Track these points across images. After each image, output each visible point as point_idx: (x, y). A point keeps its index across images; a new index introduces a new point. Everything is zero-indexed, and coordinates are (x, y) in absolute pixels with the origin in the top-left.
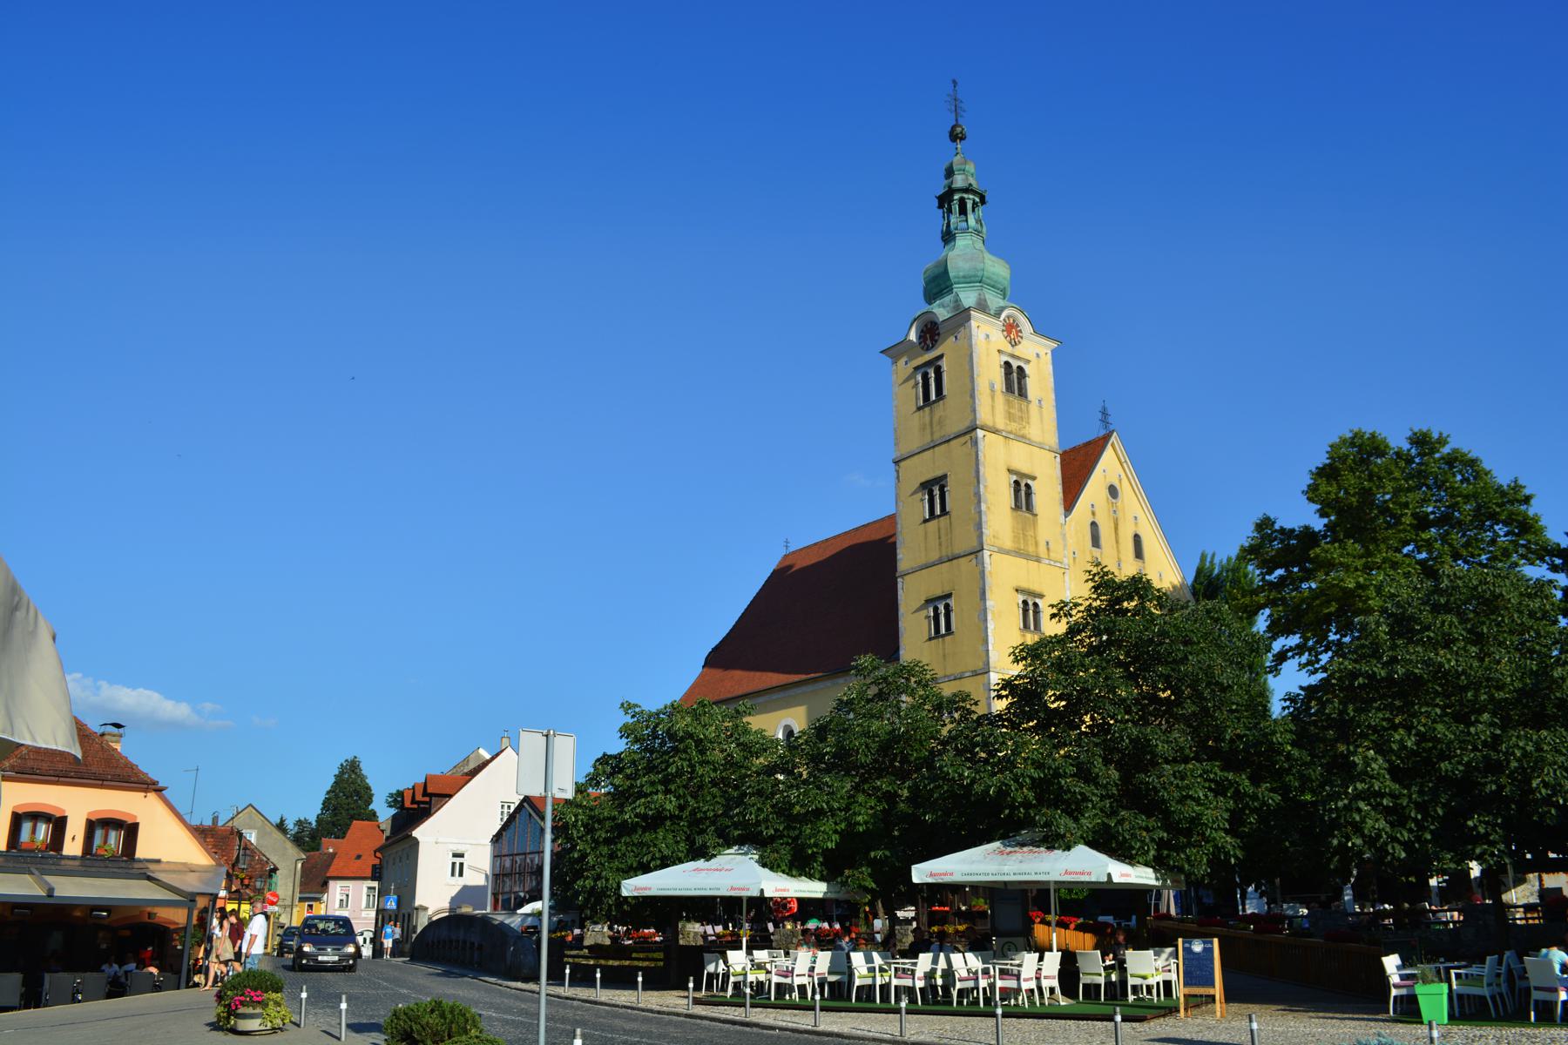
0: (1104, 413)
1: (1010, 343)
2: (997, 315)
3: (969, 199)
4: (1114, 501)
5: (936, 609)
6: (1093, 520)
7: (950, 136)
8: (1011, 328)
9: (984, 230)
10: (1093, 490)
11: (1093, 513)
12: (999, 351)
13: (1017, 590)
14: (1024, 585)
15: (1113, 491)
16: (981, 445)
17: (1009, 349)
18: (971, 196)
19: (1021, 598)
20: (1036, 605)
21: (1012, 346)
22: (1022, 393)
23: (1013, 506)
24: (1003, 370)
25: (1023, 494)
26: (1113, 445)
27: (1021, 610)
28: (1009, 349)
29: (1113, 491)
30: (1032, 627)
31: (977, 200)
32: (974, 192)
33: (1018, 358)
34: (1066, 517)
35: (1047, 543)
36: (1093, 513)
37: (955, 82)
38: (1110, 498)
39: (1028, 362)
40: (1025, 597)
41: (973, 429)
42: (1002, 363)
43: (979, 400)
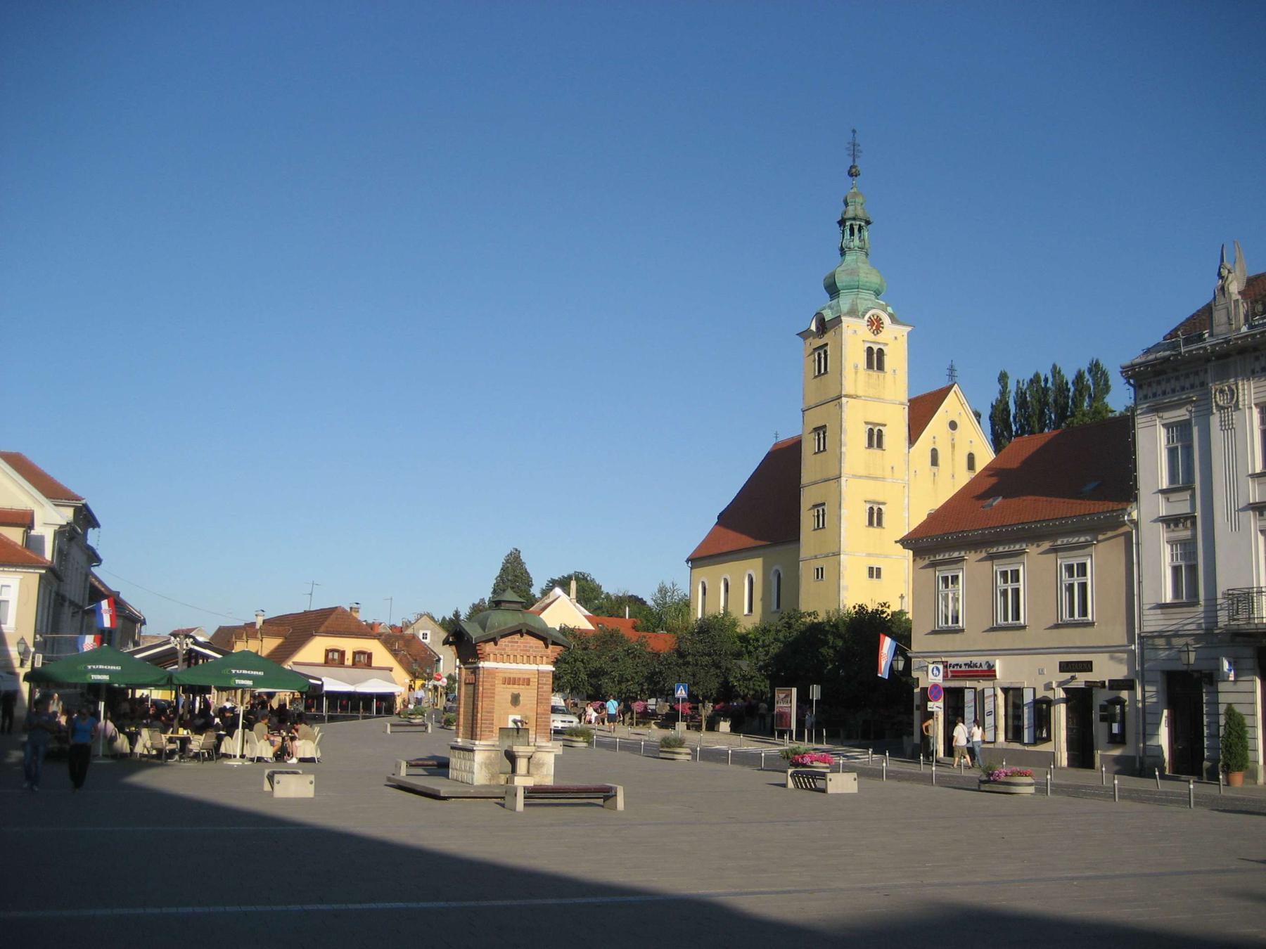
0: (952, 369)
1: (873, 333)
2: (863, 316)
3: (856, 225)
4: (954, 432)
7: (849, 173)
8: (876, 325)
9: (867, 246)
10: (937, 424)
12: (863, 341)
13: (865, 501)
15: (953, 425)
16: (845, 408)
18: (858, 223)
19: (869, 506)
20: (880, 509)
21: (875, 335)
23: (867, 446)
25: (875, 438)
26: (955, 392)
27: (867, 514)
28: (871, 337)
29: (953, 425)
30: (875, 525)
31: (863, 224)
32: (861, 220)
33: (879, 343)
34: (909, 448)
35: (892, 468)
36: (934, 443)
40: (871, 505)
41: (840, 397)
43: (845, 377)
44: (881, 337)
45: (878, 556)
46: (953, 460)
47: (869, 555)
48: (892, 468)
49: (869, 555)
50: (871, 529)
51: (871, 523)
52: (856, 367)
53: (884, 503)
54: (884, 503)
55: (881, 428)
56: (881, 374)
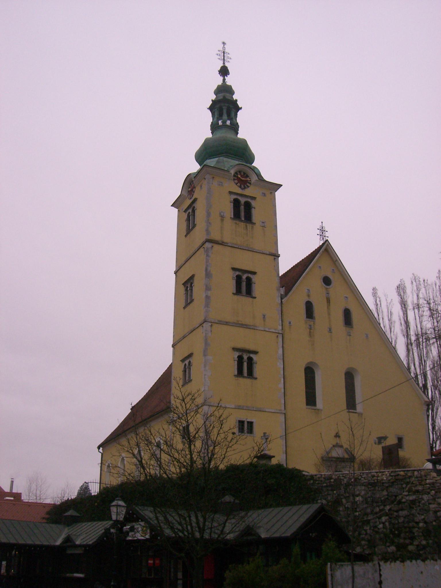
0: (322, 230)
4: (328, 287)
5: (185, 365)
6: (307, 299)
11: (309, 296)
14: (239, 346)
15: (327, 281)
17: (239, 190)
19: (237, 354)
20: (250, 359)
22: (248, 218)
23: (235, 292)
24: (232, 204)
28: (239, 190)
35: (264, 316)
36: (309, 296)
37: (224, 43)
38: (324, 285)
39: (254, 198)
40: (241, 354)
42: (232, 200)
44: (248, 192)
45: (248, 409)
46: (329, 314)
47: (239, 408)
48: (264, 316)
49: (239, 408)
50: (241, 380)
51: (240, 373)
52: (222, 218)
53: (256, 353)
54: (256, 353)
55: (250, 275)
56: (249, 226)
